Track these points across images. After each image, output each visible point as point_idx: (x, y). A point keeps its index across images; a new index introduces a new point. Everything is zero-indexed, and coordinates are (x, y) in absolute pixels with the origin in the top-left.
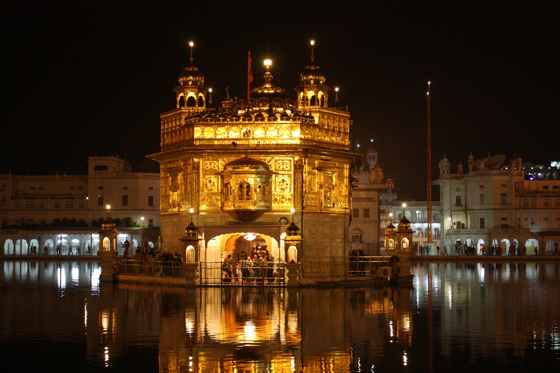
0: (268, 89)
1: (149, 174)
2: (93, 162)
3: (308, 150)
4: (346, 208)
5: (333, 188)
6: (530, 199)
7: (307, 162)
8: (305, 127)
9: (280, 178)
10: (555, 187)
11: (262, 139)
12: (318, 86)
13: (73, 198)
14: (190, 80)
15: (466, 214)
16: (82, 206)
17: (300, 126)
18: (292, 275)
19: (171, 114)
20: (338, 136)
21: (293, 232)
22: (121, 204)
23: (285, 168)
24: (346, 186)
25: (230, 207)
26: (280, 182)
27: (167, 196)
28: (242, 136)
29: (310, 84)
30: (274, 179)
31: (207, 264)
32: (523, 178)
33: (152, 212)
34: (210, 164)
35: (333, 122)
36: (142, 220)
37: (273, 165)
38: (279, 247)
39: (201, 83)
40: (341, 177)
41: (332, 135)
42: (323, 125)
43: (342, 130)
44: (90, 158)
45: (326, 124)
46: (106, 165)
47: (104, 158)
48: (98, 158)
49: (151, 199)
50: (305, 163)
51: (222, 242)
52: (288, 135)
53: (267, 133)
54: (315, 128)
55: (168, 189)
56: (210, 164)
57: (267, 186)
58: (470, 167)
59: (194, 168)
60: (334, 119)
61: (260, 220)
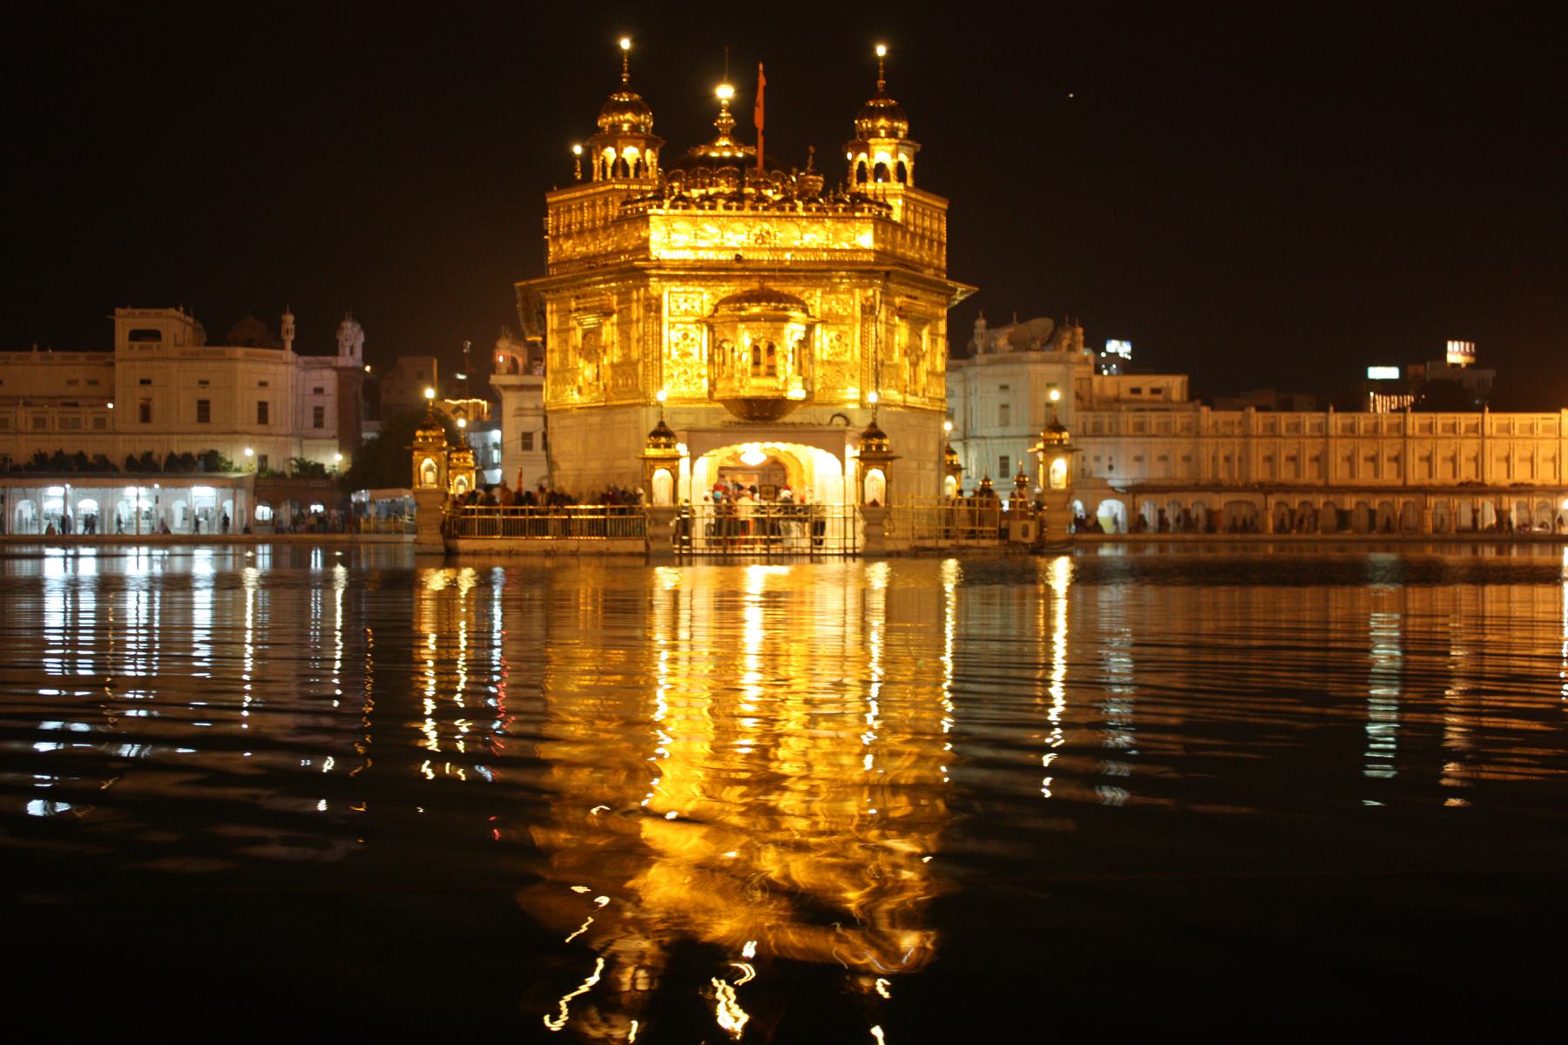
2: (126, 321)
6: (1106, 414)
10: (1155, 391)
13: (76, 405)
15: (965, 445)
16: (100, 423)
18: (875, 530)
19: (578, 194)
25: (723, 390)
28: (752, 241)
32: (1092, 369)
36: (245, 456)
40: (934, 335)
44: (119, 311)
47: (153, 311)
48: (137, 311)
58: (979, 343)
59: (648, 308)
61: (788, 418)
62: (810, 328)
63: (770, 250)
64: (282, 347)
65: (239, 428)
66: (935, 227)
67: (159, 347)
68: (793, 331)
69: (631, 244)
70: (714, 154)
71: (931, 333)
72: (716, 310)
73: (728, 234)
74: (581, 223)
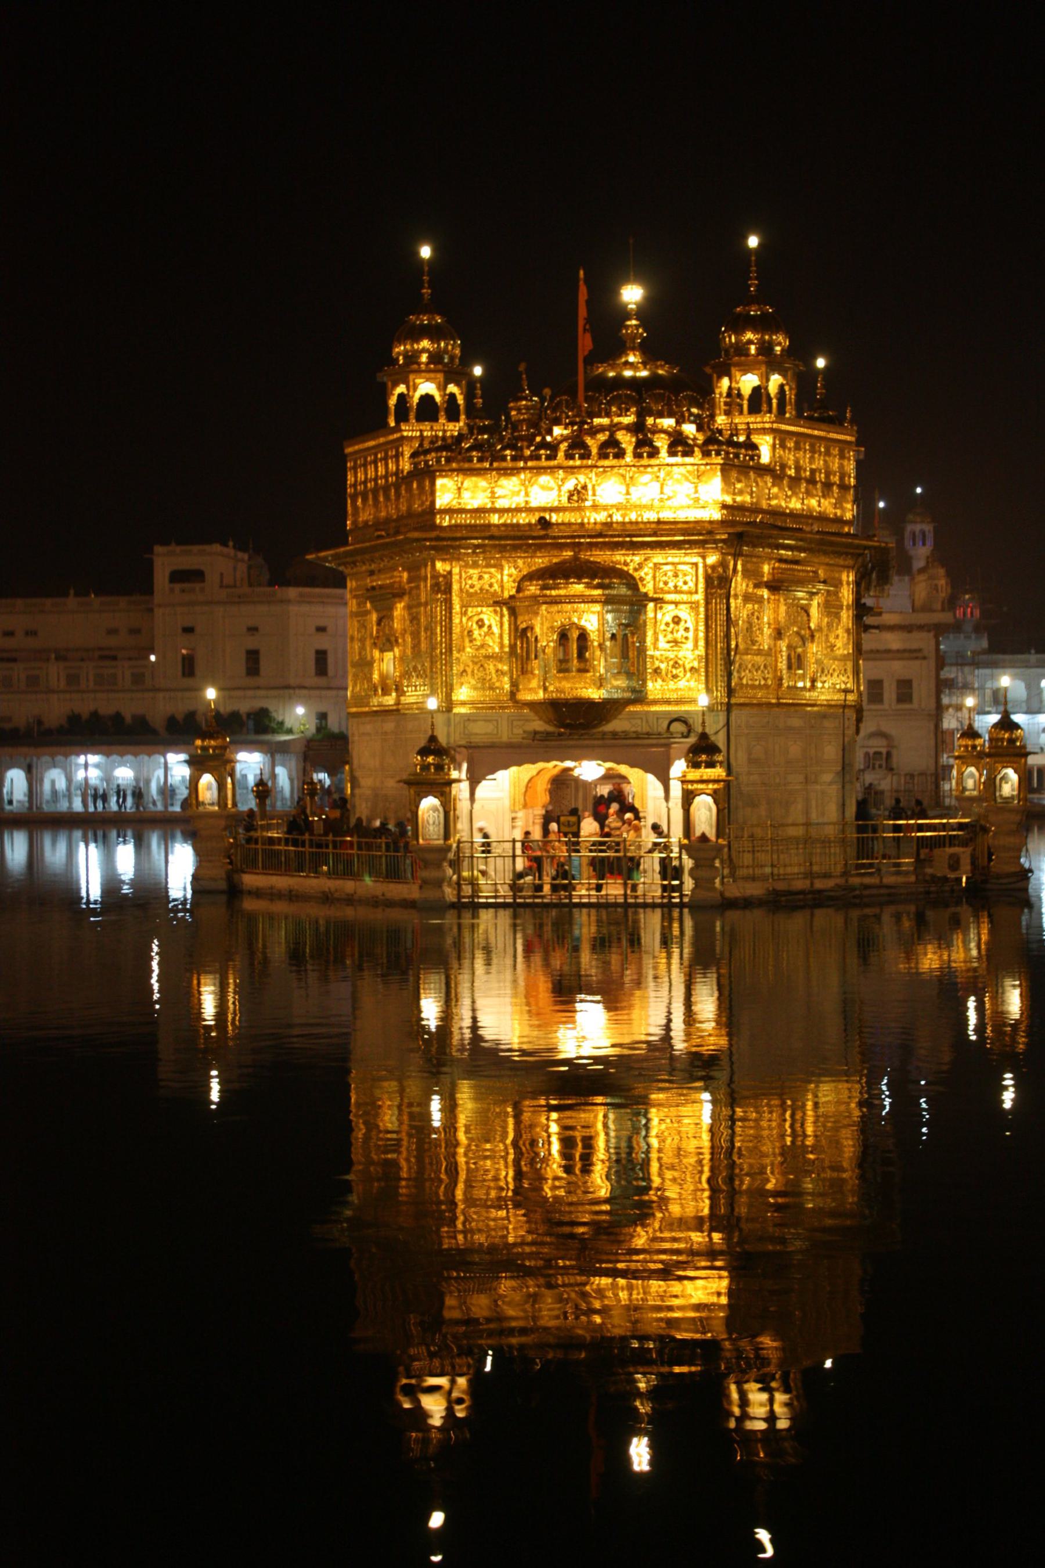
0: (634, 367)
1: (317, 590)
2: (165, 560)
3: (742, 534)
4: (846, 691)
5: (812, 636)
7: (739, 567)
8: (734, 474)
9: (668, 612)
12: (769, 362)
13: (115, 658)
14: (424, 350)
16: (138, 679)
17: (723, 471)
18: (702, 873)
19: (372, 443)
20: (824, 496)
21: (704, 757)
22: (244, 671)
23: (680, 584)
24: (848, 631)
25: (534, 692)
26: (667, 624)
27: (366, 665)
29: (747, 354)
30: (650, 614)
33: (324, 692)
34: (480, 578)
35: (812, 458)
36: (298, 715)
37: (649, 578)
38: (667, 798)
39: (452, 358)
40: (831, 608)
41: (809, 494)
42: (783, 466)
43: (836, 479)
44: (158, 549)
45: (791, 463)
46: (202, 568)
47: (195, 548)
48: (178, 549)
49: (321, 657)
50: (735, 570)
51: (515, 785)
53: (632, 490)
54: (761, 476)
55: (368, 643)
56: (480, 578)
57: (633, 634)
59: (436, 588)
60: (813, 451)
61: (616, 725)
65: (292, 682)
66: (835, 466)
67: (202, 590)
72: (519, 590)
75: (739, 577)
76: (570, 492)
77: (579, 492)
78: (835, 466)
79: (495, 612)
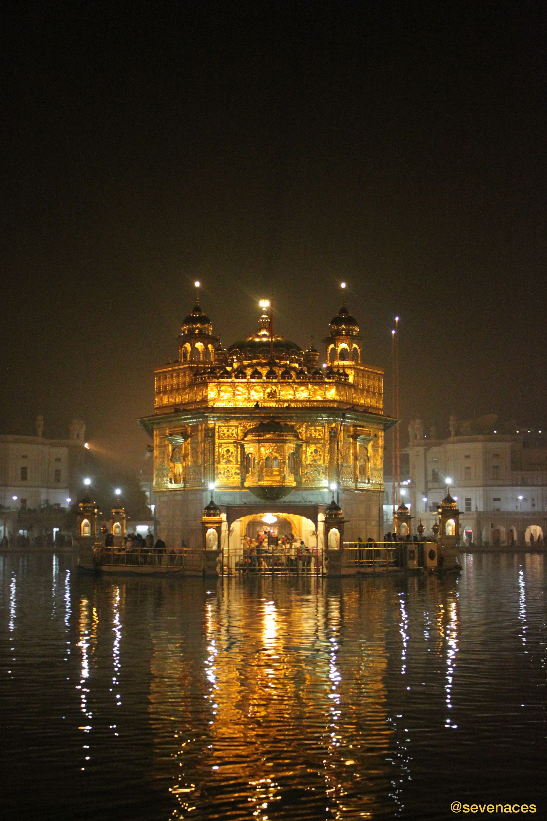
4: (381, 485)
5: (369, 460)
7: (342, 428)
8: (341, 388)
9: (313, 448)
11: (291, 401)
14: (197, 328)
19: (170, 369)
23: (317, 435)
24: (381, 458)
28: (266, 396)
30: (304, 449)
31: (231, 551)
34: (228, 431)
35: (368, 381)
41: (367, 397)
42: (358, 385)
43: (377, 390)
52: (321, 396)
53: (296, 393)
56: (228, 431)
59: (206, 436)
61: (288, 498)
62: (299, 447)
63: (277, 401)
64: (35, 433)
66: (376, 385)
68: (290, 447)
69: (199, 398)
70: (257, 340)
71: (373, 446)
73: (253, 392)
74: (172, 386)
75: (342, 433)
76: (268, 393)
77: (272, 394)
78: (376, 385)
79: (235, 446)
